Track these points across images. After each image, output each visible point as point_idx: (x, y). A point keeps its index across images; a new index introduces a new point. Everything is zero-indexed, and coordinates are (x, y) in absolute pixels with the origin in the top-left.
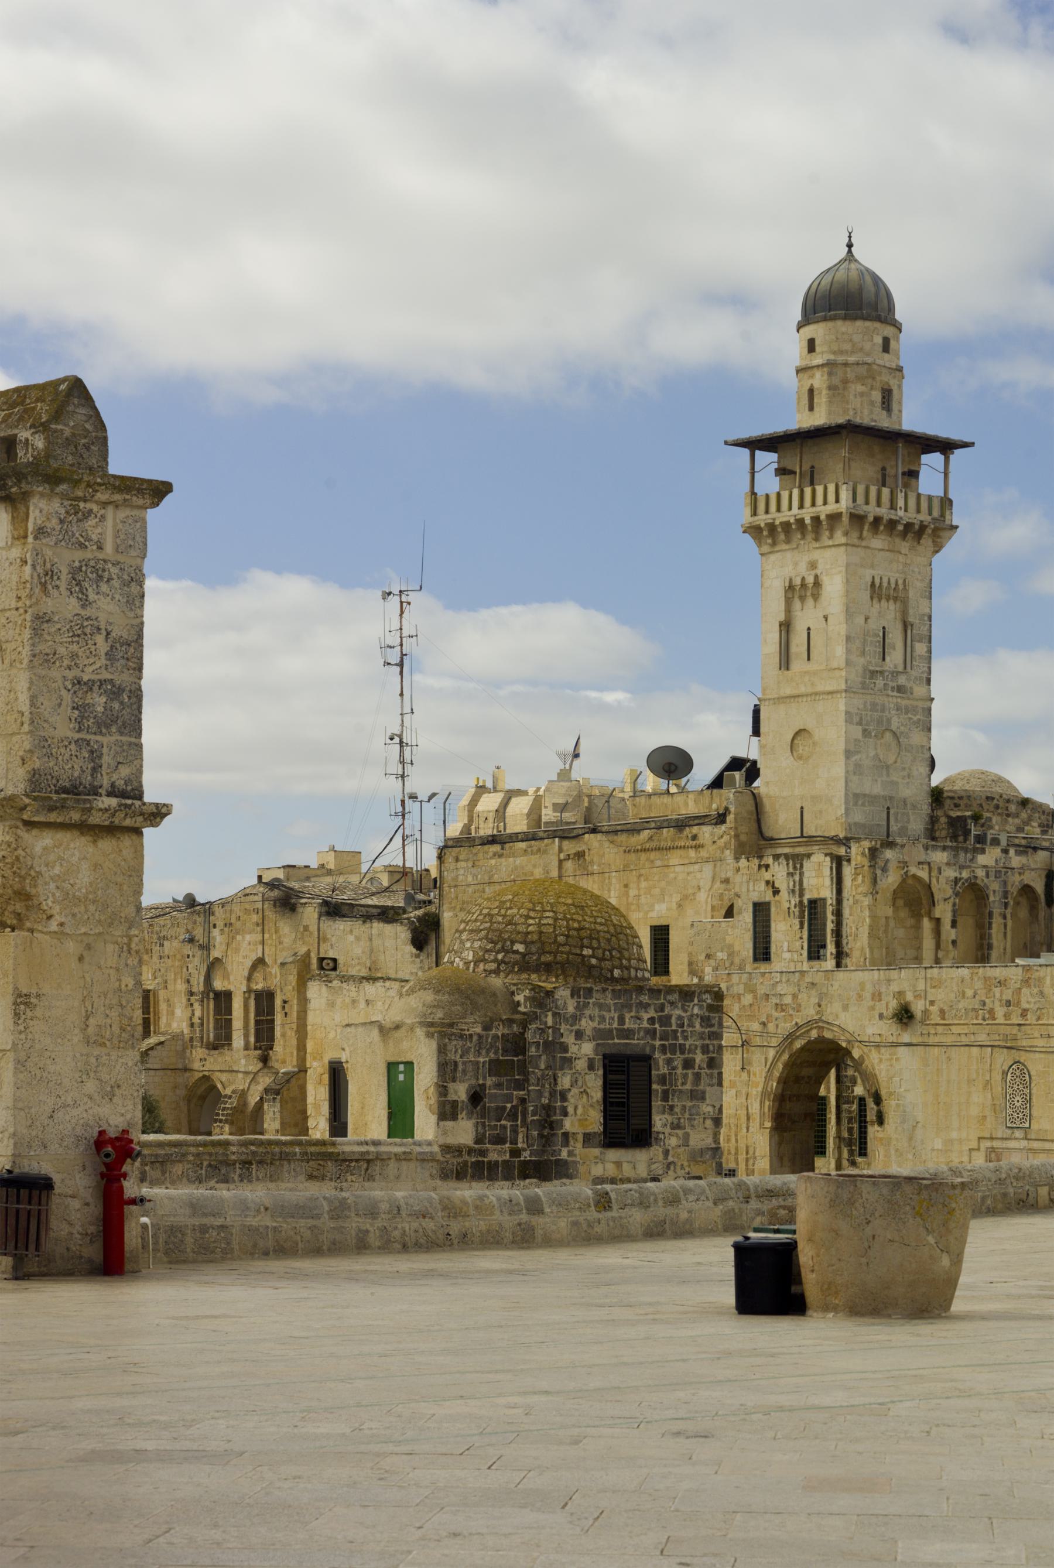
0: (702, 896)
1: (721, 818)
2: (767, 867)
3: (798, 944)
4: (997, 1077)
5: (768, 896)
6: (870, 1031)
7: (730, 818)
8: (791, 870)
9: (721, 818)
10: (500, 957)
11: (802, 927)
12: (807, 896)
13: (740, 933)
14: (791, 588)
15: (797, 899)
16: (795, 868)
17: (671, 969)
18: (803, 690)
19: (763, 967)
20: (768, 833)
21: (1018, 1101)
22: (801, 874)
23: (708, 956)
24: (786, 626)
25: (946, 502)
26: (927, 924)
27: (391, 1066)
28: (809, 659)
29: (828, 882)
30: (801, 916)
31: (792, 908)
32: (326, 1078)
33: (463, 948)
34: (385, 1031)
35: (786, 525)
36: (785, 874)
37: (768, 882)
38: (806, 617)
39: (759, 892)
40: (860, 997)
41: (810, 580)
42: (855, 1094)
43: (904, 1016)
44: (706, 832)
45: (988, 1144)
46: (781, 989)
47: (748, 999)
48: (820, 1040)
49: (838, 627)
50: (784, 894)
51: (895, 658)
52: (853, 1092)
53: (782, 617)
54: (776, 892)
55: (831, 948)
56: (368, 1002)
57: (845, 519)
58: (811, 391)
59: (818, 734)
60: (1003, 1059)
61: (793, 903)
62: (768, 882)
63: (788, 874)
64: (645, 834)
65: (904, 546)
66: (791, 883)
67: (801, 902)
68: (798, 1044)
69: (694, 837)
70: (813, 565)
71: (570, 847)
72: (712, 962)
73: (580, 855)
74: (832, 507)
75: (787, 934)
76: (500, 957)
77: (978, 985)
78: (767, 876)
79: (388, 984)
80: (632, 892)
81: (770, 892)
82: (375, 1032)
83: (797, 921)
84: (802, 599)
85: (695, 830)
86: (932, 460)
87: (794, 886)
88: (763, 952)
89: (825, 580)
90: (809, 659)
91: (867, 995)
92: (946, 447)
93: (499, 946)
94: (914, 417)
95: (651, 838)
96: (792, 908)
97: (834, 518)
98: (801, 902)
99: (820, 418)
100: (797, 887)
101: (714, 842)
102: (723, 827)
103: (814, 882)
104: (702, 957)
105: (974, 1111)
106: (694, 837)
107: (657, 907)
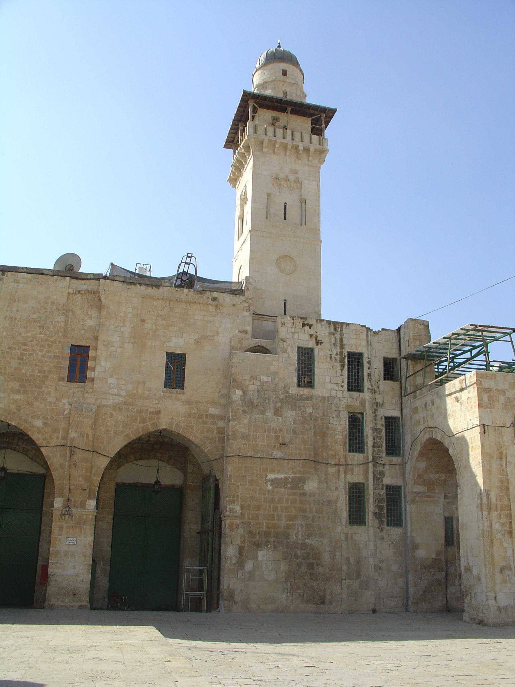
2: (310, 326)
8: (332, 330)
15: (339, 350)
16: (336, 329)
17: (186, 384)
22: (342, 335)
23: (253, 378)
28: (285, 219)
30: (342, 361)
31: (334, 355)
36: (327, 333)
37: (311, 336)
42: (384, 482)
50: (326, 344)
52: (382, 481)
54: (318, 343)
61: (335, 352)
62: (311, 336)
63: (330, 333)
66: (333, 340)
67: (341, 353)
70: (295, 172)
78: (311, 331)
80: (148, 326)
83: (338, 364)
85: (215, 295)
87: (335, 341)
90: (285, 219)
96: (334, 355)
98: (341, 353)
100: (338, 342)
101: (234, 305)
103: (353, 341)
104: (248, 377)
106: (214, 299)
107: (174, 340)
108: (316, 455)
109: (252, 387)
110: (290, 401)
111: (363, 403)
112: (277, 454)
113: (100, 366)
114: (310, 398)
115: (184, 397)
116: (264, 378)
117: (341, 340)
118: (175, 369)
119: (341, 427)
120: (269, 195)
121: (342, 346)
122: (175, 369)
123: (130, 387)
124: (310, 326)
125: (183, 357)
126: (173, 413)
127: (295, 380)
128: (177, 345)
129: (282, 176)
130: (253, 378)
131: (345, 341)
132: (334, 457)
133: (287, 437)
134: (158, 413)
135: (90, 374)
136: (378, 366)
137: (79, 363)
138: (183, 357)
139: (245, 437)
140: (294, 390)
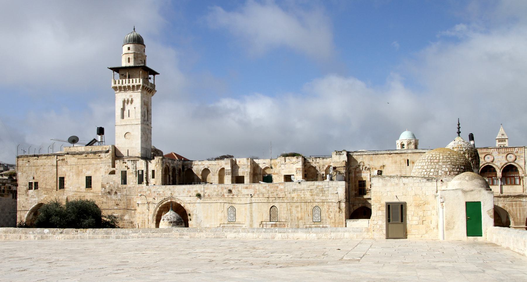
0: (102, 170)
1: (107, 152)
2: (125, 163)
3: (135, 181)
4: (226, 209)
5: (126, 169)
6: (187, 200)
7: (110, 152)
9: (107, 152)
10: (458, 170)
13: (117, 178)
14: (124, 102)
17: (92, 186)
18: (128, 123)
19: (124, 186)
20: (118, 155)
21: (232, 215)
23: (107, 183)
24: (123, 109)
25: (154, 86)
26: (168, 176)
27: (467, 204)
29: (144, 166)
32: (384, 209)
33: (442, 167)
34: (464, 192)
35: (125, 87)
38: (128, 107)
40: (184, 192)
41: (130, 99)
43: (199, 196)
44: (103, 155)
45: (223, 225)
46: (159, 190)
47: (149, 192)
48: (171, 202)
49: (139, 110)
51: (146, 117)
53: (122, 107)
54: (128, 168)
55: (145, 181)
56: (404, 184)
57: (141, 87)
58: (129, 59)
59: (132, 133)
60: (227, 206)
64: (84, 155)
65: (148, 94)
68: (164, 203)
69: (99, 156)
70: (131, 96)
71: (61, 158)
73: (63, 160)
74: (138, 83)
75: (132, 179)
76: (458, 170)
77: (220, 189)
78: (126, 165)
79: (415, 178)
81: (126, 168)
82: (460, 193)
84: (128, 103)
85: (100, 154)
86: (151, 76)
89: (134, 99)
91: (186, 191)
92: (154, 73)
93: (457, 167)
94: (148, 65)
95: (86, 156)
97: (138, 86)
99: (132, 64)
102: (108, 154)
103: (140, 166)
105: (219, 218)
106: (99, 156)
108: (127, 207)
109: (107, 186)
112: (116, 208)
113: (67, 184)
114: (125, 188)
115: (92, 191)
116: (111, 183)
118: (89, 182)
122: (89, 182)
123: (76, 189)
124: (125, 163)
126: (89, 196)
128: (88, 174)
130: (107, 183)
132: (133, 207)
133: (118, 202)
134: (84, 196)
135: (65, 186)
136: (150, 173)
137: (61, 183)
139: (106, 203)
140: (120, 186)
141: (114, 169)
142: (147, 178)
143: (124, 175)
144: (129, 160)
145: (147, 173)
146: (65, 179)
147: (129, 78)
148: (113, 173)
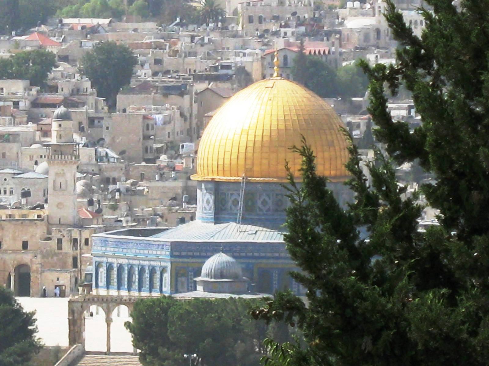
5: (62, 237)
11: (71, 243)
12: (73, 238)
13: (53, 243)
19: (60, 251)
20: (50, 222)
23: (44, 248)
39: (59, 236)
50: (66, 236)
54: (64, 237)
62: (61, 235)
70: (63, 170)
72: (45, 249)
80: (17, 234)
88: (60, 248)
104: (43, 248)
106: (35, 224)
110: (55, 254)
111: (77, 254)
114: (61, 253)
117: (71, 235)
119: (70, 261)
120: (54, 181)
121: (71, 237)
125: (27, 242)
127: (57, 248)
128: (25, 238)
129: (59, 173)
130: (44, 248)
131: (72, 235)
136: (83, 241)
138: (27, 242)
140: (56, 251)
141: (50, 236)
142: (80, 245)
143: (60, 241)
144: (64, 230)
145: (80, 241)
146: (2, 243)
147: (61, 154)
148: (50, 239)
